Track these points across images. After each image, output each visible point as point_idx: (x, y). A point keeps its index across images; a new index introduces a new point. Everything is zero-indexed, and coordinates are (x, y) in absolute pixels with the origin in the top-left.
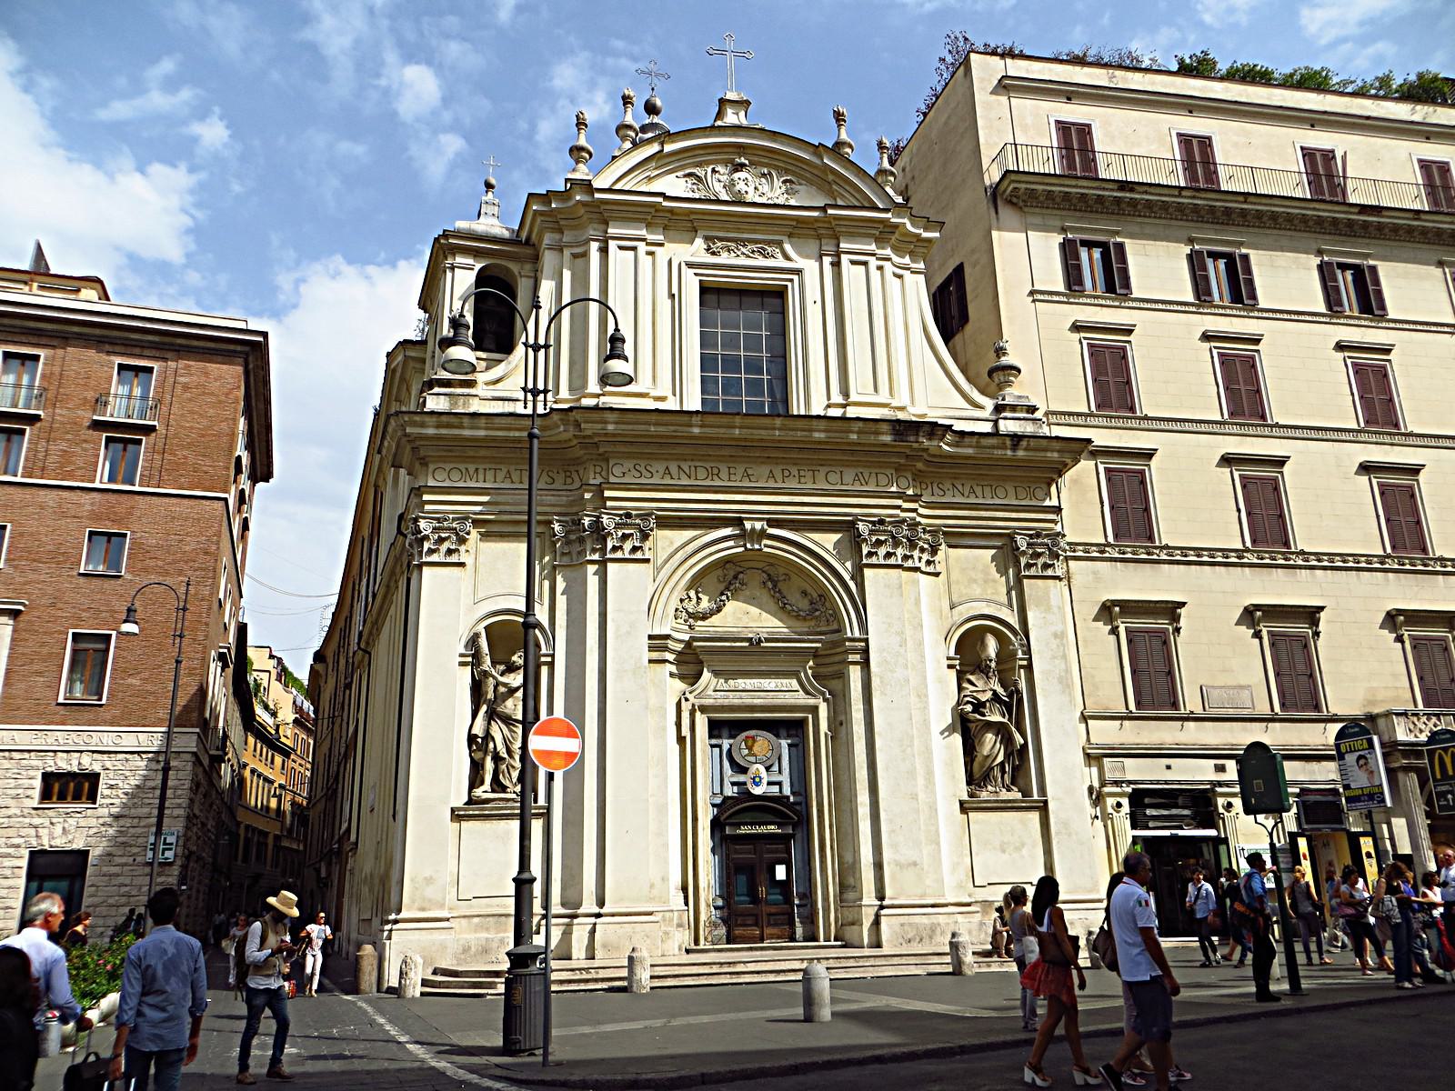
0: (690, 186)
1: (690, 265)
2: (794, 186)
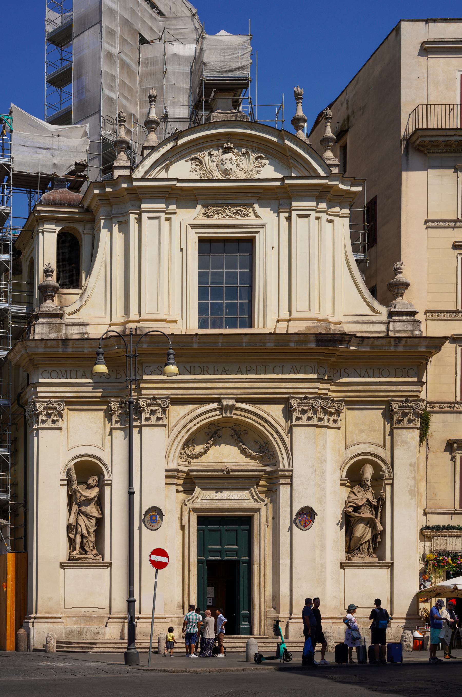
0: (194, 167)
1: (193, 227)
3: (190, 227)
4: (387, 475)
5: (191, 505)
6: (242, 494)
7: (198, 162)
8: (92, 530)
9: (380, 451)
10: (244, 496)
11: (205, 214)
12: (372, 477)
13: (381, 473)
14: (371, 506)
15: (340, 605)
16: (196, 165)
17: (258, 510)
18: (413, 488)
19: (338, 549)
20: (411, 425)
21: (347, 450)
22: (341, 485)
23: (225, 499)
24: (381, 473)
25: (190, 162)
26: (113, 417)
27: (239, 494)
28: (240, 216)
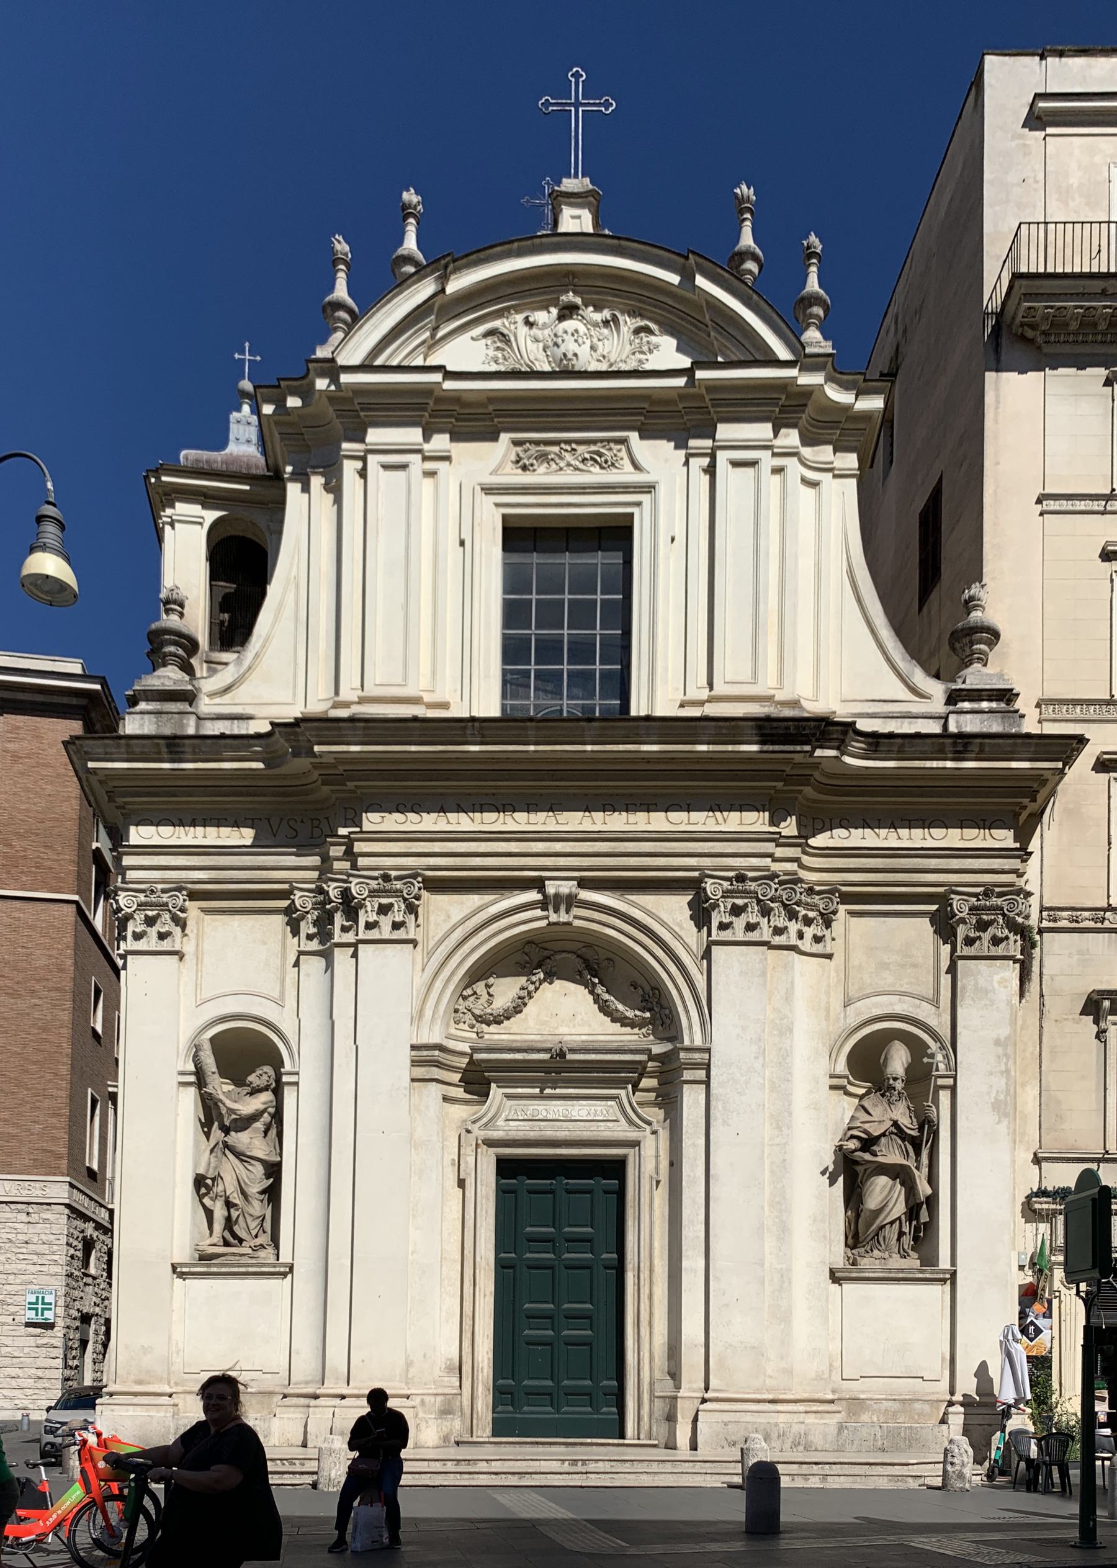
0: (491, 353)
1: (488, 490)
2: (653, 339)
3: (482, 489)
4: (942, 1066)
5: (482, 1133)
6: (599, 1108)
7: (501, 341)
8: (254, 1189)
9: (925, 1013)
10: (605, 1112)
11: (518, 462)
12: (907, 1070)
13: (925, 1060)
14: (903, 1140)
15: (831, 1370)
16: (498, 349)
17: (635, 1144)
18: (1002, 1097)
19: (825, 1237)
20: (1000, 950)
21: (848, 1008)
22: (832, 1087)
23: (562, 1118)
24: (925, 1060)
25: (484, 341)
26: (303, 924)
27: (593, 1108)
28: (598, 467)
